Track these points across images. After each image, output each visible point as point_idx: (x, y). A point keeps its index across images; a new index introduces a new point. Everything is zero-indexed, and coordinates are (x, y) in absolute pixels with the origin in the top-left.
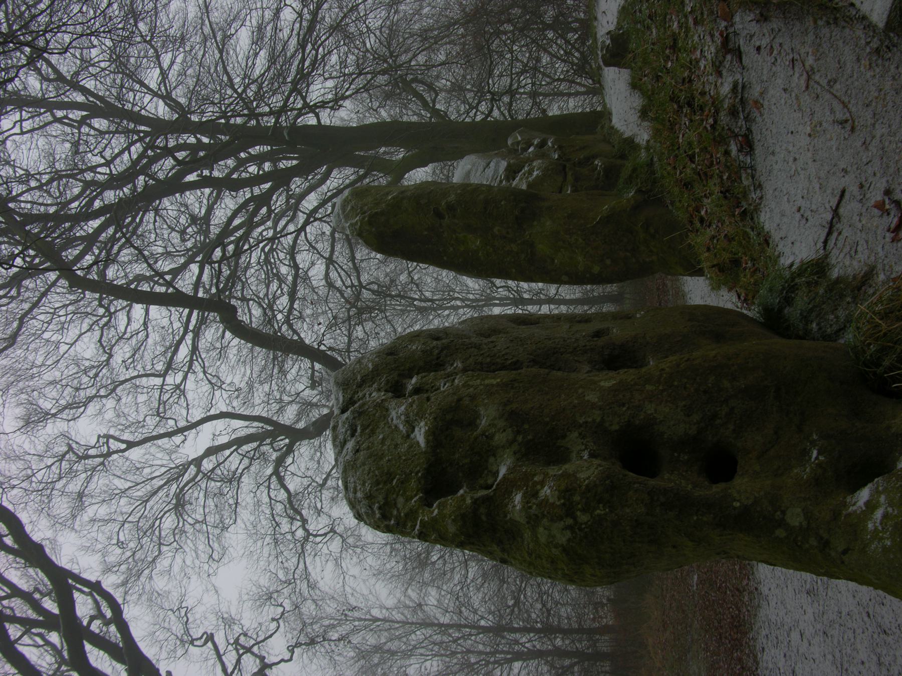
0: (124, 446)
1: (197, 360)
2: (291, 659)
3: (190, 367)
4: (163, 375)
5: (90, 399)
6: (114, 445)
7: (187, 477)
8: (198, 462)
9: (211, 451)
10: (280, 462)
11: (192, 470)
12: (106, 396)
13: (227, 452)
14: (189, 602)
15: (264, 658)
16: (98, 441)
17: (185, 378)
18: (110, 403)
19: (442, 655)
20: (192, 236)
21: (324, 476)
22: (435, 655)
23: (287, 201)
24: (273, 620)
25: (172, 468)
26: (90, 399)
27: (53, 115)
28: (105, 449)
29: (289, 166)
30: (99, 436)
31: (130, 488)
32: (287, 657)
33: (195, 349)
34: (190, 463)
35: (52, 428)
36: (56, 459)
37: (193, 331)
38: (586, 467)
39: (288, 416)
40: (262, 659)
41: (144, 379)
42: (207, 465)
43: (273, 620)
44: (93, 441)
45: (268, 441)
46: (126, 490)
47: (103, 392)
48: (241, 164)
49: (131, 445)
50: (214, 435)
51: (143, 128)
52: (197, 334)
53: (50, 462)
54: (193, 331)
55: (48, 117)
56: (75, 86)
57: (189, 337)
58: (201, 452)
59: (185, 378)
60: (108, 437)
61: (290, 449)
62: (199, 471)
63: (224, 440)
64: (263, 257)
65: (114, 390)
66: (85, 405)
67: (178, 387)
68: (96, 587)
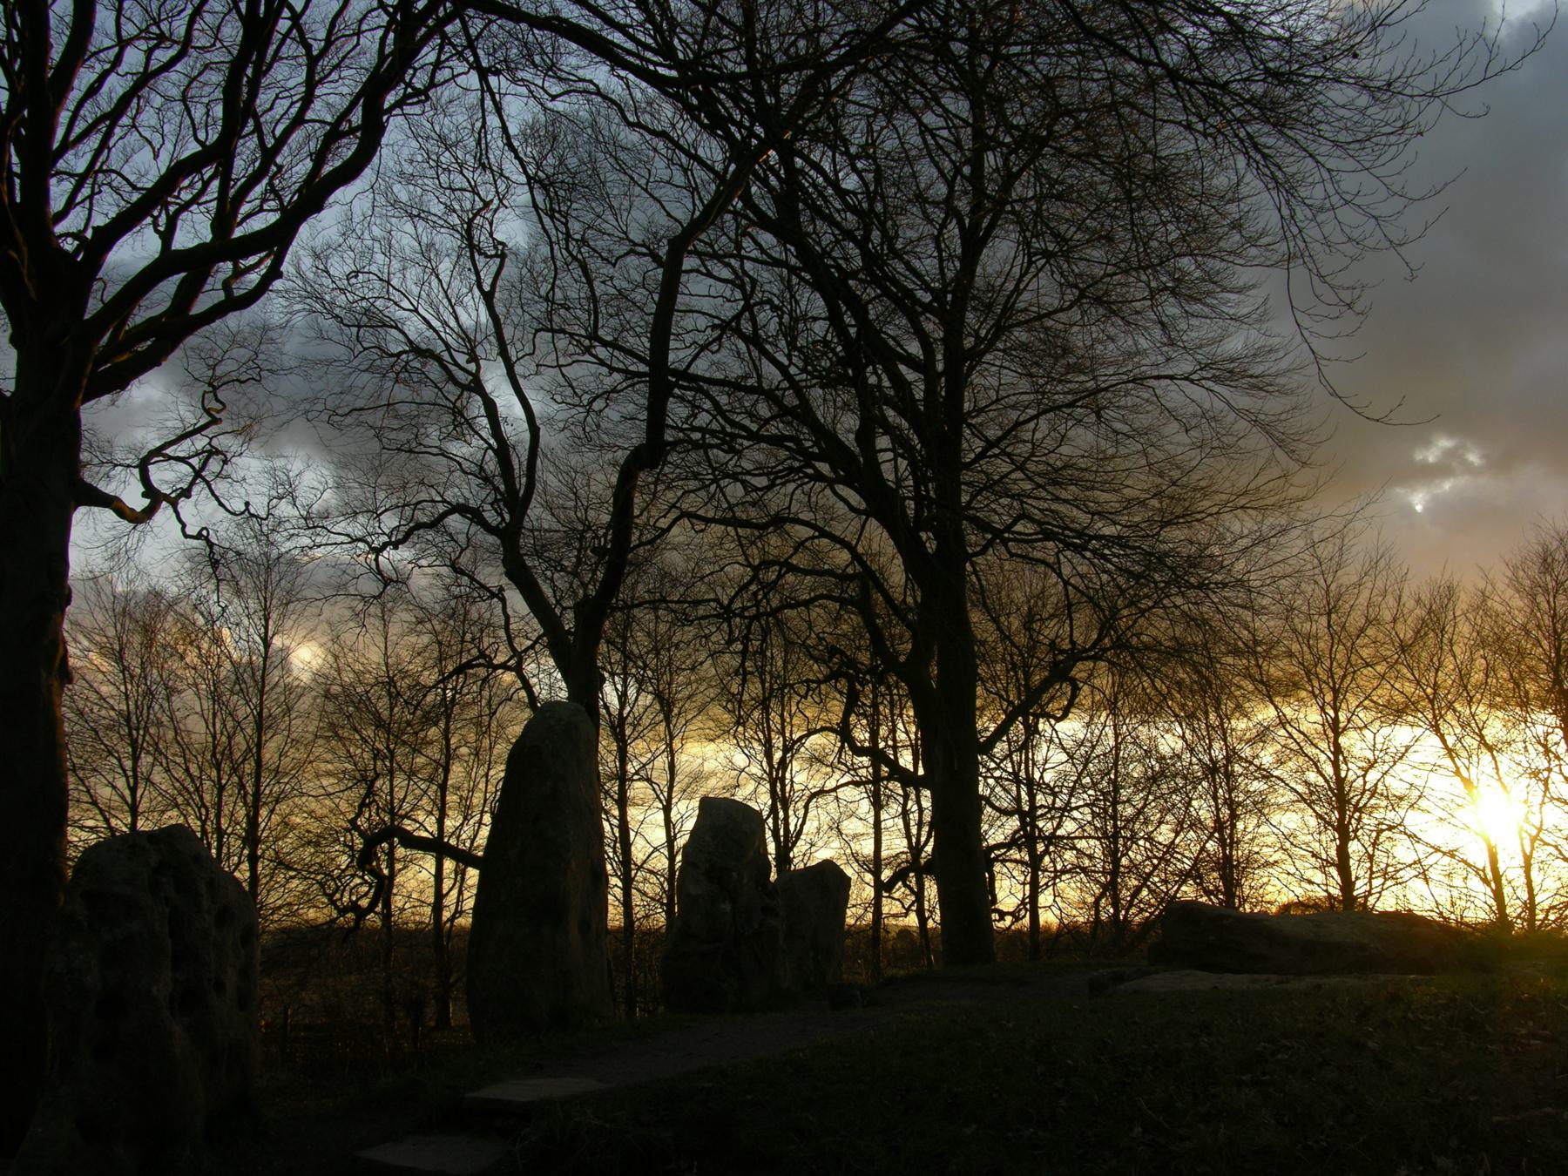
2: (186, 536)
8: (476, 386)
9: (490, 407)
14: (269, 382)
15: (189, 497)
19: (215, 747)
22: (214, 737)
24: (247, 504)
32: (191, 531)
40: (186, 493)
43: (247, 504)
46: (437, 276)
49: (488, 297)
63: (507, 430)
68: (275, 273)
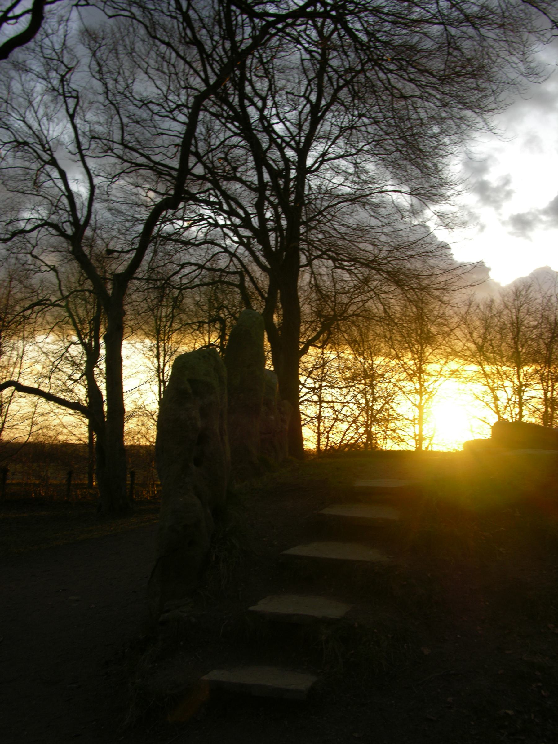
0: (71, 111)
1: (131, 167)
3: (126, 161)
4: (123, 143)
5: (105, 85)
10: (54, 226)
11: (46, 157)
23: (245, 237)
25: (46, 137)
29: (271, 239)
33: (140, 165)
34: (51, 155)
37: (154, 166)
38: (200, 424)
39: (88, 232)
44: (73, 86)
45: (71, 219)
48: (275, 207)
51: (303, 139)
52: (151, 168)
59: (119, 157)
60: (77, 97)
61: (62, 233)
67: (112, 150)
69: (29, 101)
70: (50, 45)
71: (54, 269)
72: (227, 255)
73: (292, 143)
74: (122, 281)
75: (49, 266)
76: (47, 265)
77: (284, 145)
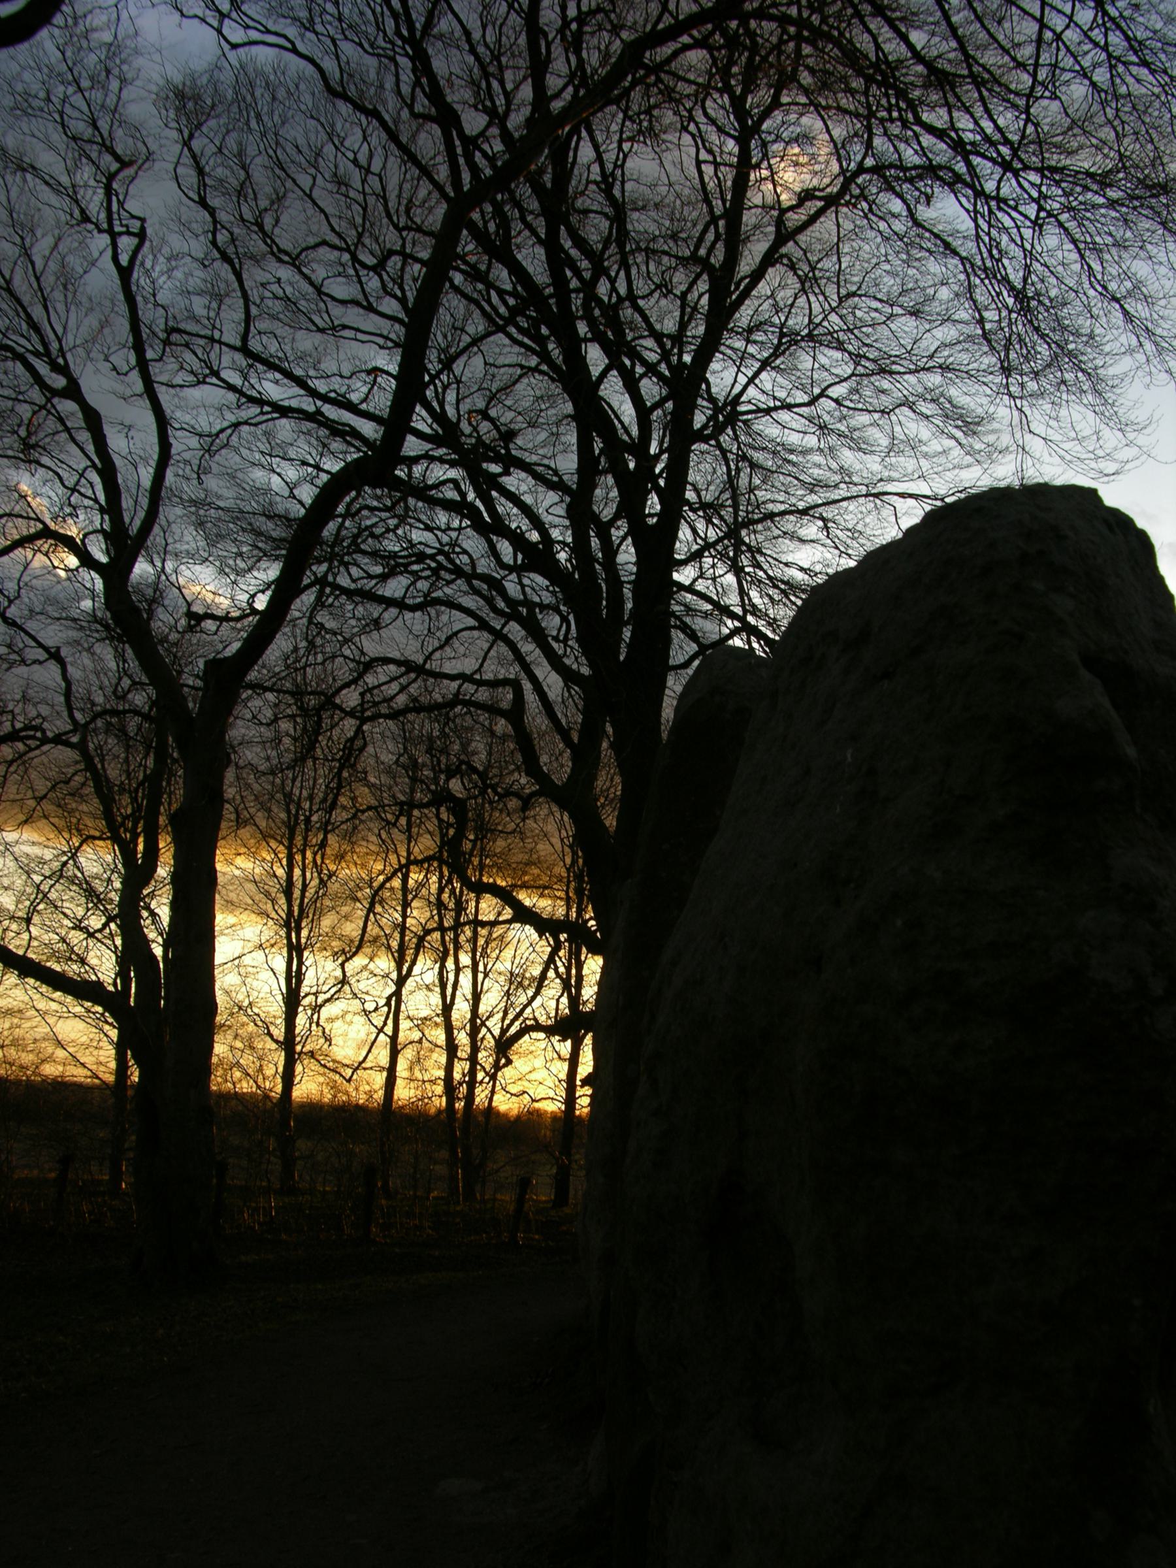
0: (124, 260)
1: (262, 413)
6: (126, 243)
7: (43, 368)
8: (73, 391)
12: (214, 243)
13: (90, 448)
16: (133, 217)
17: (231, 388)
18: (199, 247)
20: (475, 429)
21: (18, 621)
25: (60, 341)
26: (212, 212)
27: (720, 217)
28: (118, 229)
30: (143, 220)
31: (33, 264)
33: (284, 411)
35: (166, 142)
36: (106, 134)
41: (240, 315)
42: (68, 406)
44: (132, 206)
46: (29, 257)
47: (222, 237)
49: (125, 273)
50: (130, 427)
53: (104, 125)
54: (319, 412)
55: (719, 208)
56: (769, 260)
57: (308, 405)
58: (92, 400)
59: (231, 388)
60: (142, 236)
62: (55, 393)
63: (116, 442)
64: (429, 551)
65: (225, 258)
66: (203, 203)
67: (216, 374)
69: (23, 246)
70: (85, 109)
71: (55, 655)
72: (486, 634)
73: (663, 368)
74: (227, 678)
75: (46, 649)
76: (40, 645)
77: (639, 370)
